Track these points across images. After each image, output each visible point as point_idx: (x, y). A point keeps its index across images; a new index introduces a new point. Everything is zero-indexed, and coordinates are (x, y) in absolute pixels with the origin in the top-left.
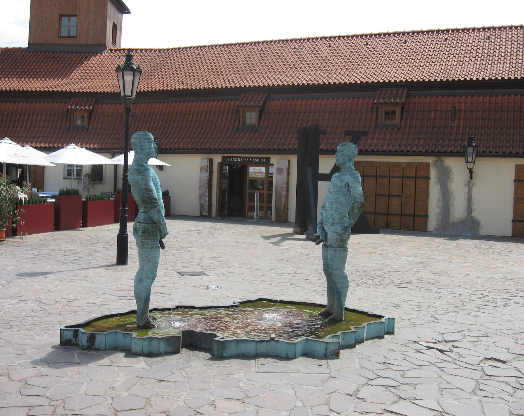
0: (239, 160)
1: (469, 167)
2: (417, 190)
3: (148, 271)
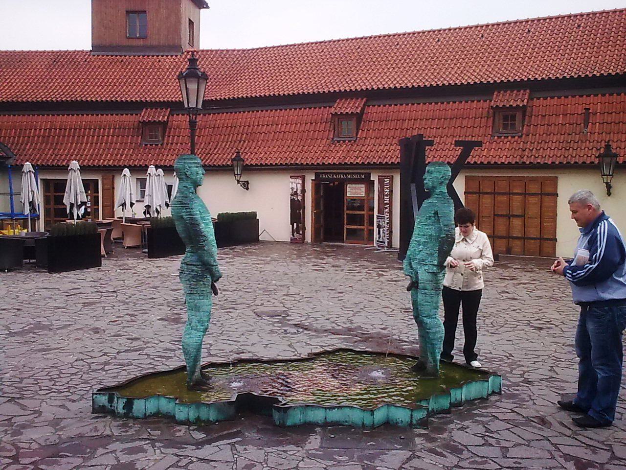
0: (335, 176)
1: (605, 181)
2: (544, 209)
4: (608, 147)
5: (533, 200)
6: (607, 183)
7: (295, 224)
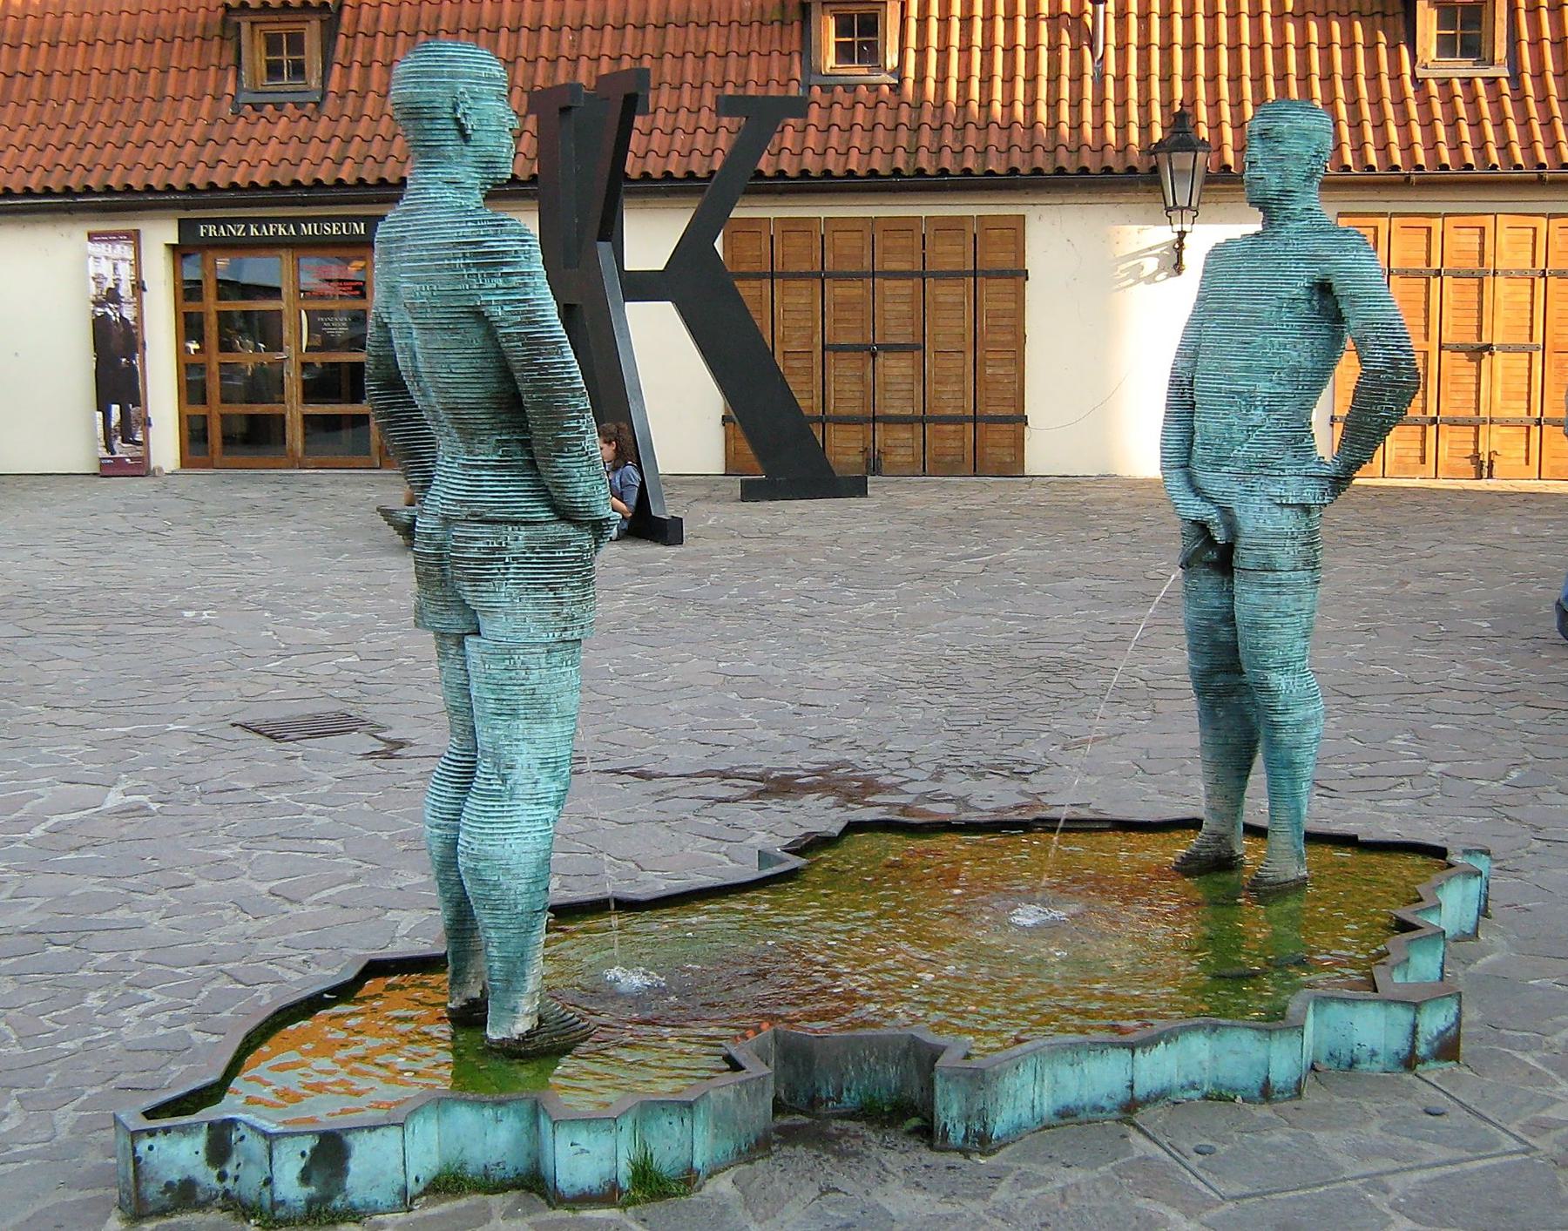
0: (253, 231)
2: (984, 322)
3: (536, 763)
5: (945, 293)
7: (115, 409)
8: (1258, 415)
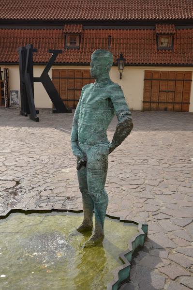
4: (121, 55)
6: (121, 73)
8: (93, 131)
